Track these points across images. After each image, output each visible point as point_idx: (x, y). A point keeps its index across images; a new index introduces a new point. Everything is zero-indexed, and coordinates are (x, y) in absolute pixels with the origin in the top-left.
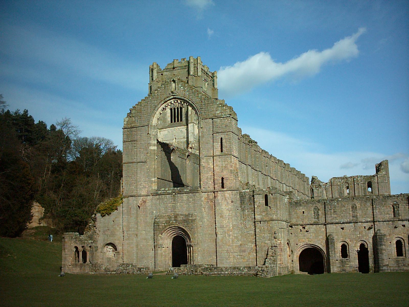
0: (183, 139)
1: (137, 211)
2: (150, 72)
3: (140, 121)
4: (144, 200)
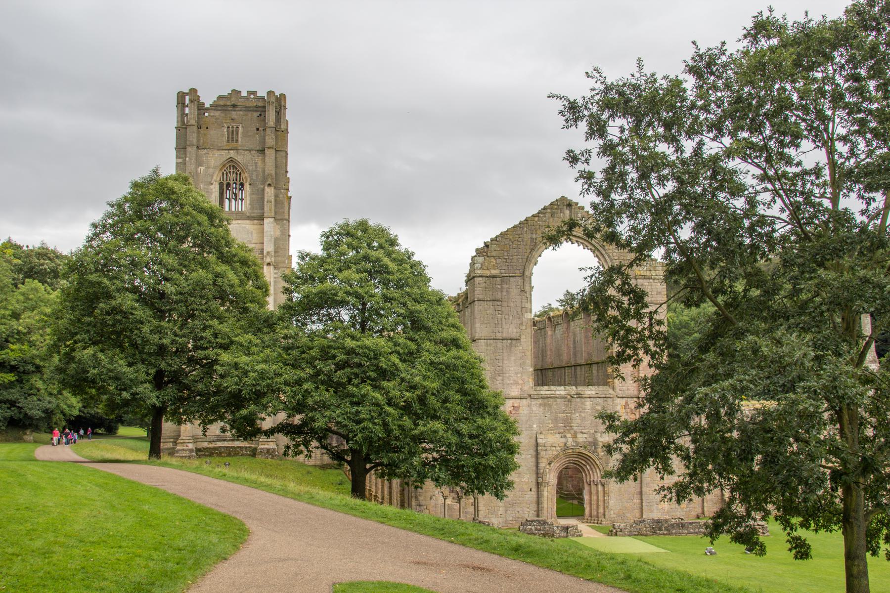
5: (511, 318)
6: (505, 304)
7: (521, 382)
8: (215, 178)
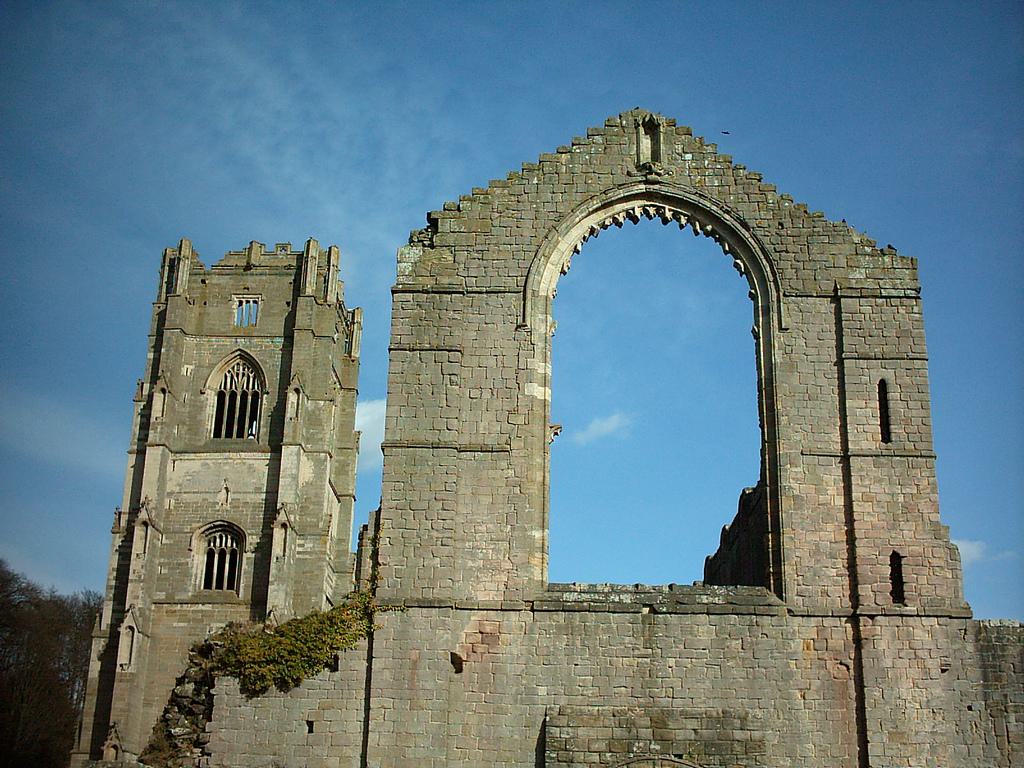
0: (252, 496)
2: (163, 267)
3: (479, 266)
4: (488, 629)
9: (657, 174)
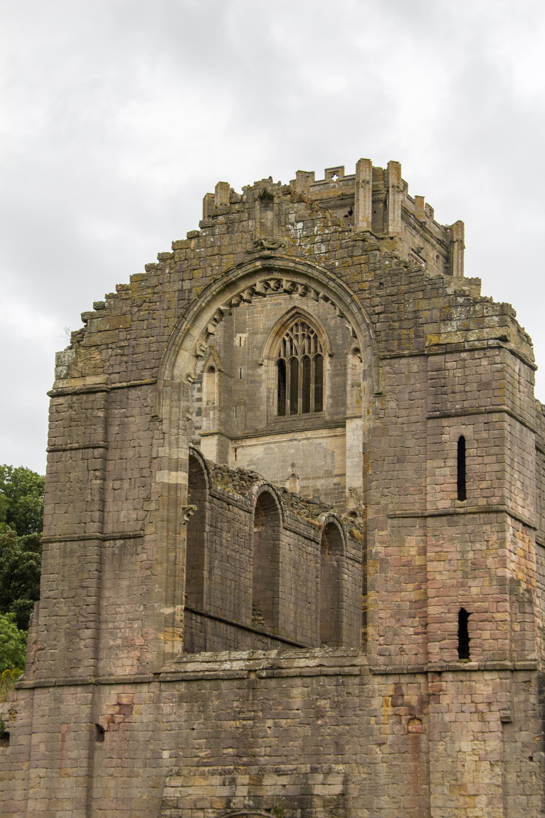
0: (322, 481)
1: (92, 750)
4: (125, 701)
5: (126, 485)
6: (114, 454)
7: (139, 641)
8: (265, 353)
9: (269, 249)
